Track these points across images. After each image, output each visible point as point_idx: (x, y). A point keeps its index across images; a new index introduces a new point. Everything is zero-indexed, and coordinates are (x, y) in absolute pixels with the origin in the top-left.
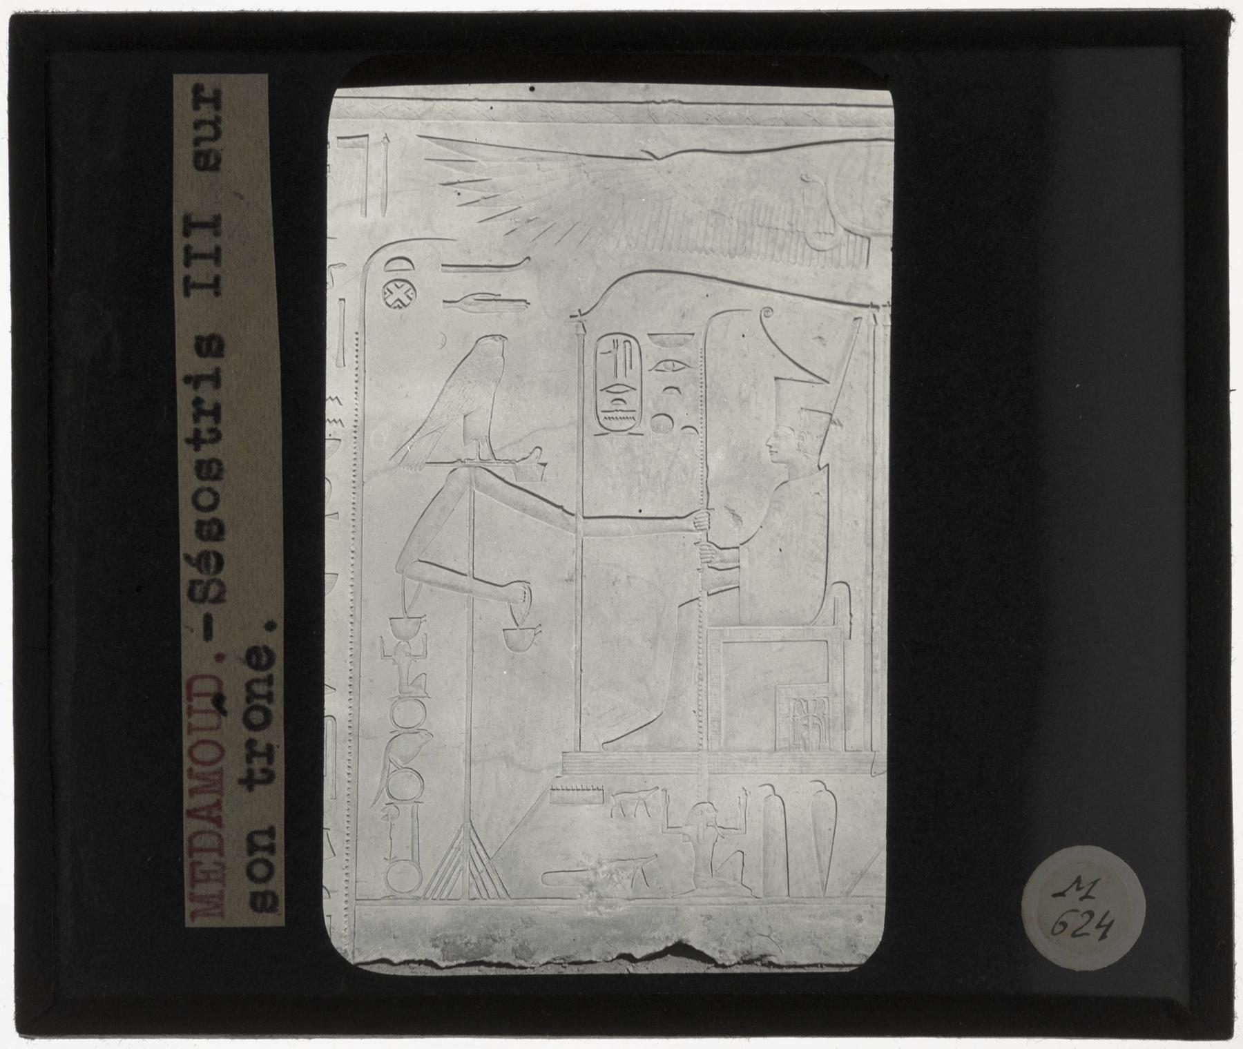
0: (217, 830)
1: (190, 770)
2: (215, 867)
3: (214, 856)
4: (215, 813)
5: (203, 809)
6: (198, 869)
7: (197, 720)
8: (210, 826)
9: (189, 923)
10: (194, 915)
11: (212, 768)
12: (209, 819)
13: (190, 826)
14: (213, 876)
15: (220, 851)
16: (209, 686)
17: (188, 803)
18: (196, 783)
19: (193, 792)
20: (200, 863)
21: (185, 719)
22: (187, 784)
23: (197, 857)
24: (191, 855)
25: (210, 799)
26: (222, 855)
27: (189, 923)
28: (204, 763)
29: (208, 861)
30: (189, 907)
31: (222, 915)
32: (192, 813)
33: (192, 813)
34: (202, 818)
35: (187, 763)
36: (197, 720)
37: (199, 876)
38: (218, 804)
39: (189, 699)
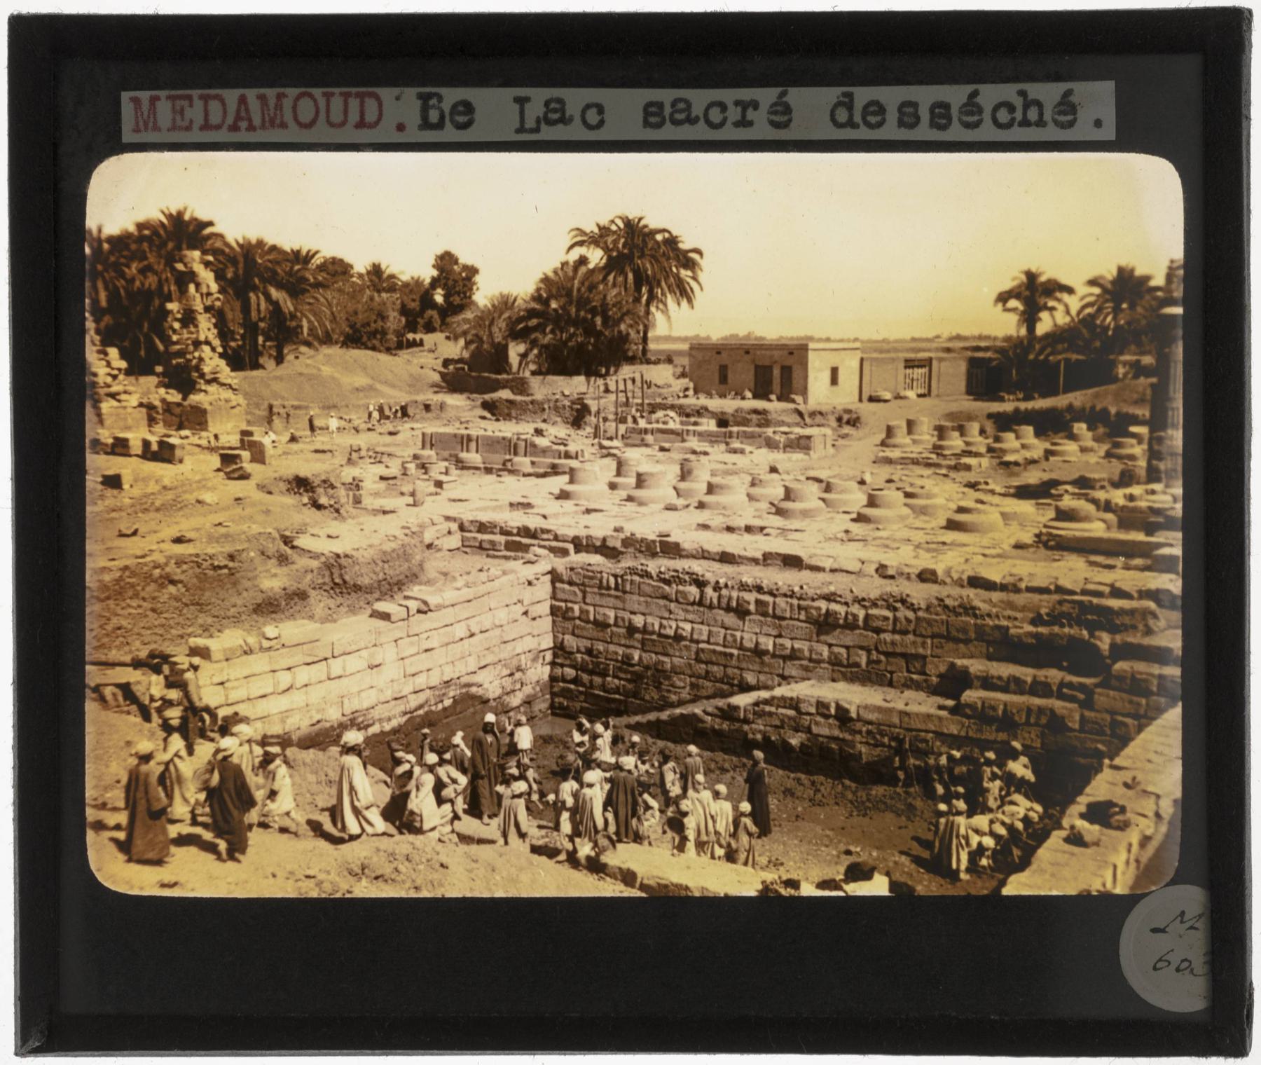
0: (226, 126)
1: (284, 95)
2: (186, 123)
3: (199, 120)
4: (244, 125)
5: (247, 110)
6: (185, 103)
7: (337, 103)
8: (230, 120)
9: (125, 96)
10: (136, 101)
11: (288, 116)
12: (238, 118)
13: (232, 96)
14: (178, 118)
15: (206, 126)
16: (371, 116)
17: (251, 94)
18: (272, 102)
19: (262, 98)
20: (191, 106)
21: (337, 90)
22: (271, 93)
23: (199, 104)
24: (201, 97)
25: (257, 121)
26: (202, 128)
27: (125, 96)
28: (294, 108)
29: (195, 113)
30: (144, 95)
31: (137, 130)
32: (243, 100)
33: (243, 100)
34: (239, 106)
35: (292, 92)
36: (337, 103)
37: (179, 103)
38: (251, 128)
39: (358, 95)
